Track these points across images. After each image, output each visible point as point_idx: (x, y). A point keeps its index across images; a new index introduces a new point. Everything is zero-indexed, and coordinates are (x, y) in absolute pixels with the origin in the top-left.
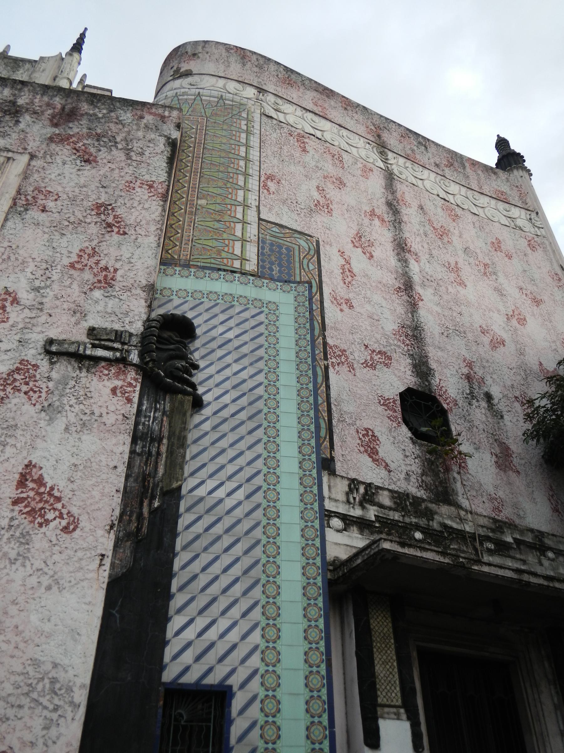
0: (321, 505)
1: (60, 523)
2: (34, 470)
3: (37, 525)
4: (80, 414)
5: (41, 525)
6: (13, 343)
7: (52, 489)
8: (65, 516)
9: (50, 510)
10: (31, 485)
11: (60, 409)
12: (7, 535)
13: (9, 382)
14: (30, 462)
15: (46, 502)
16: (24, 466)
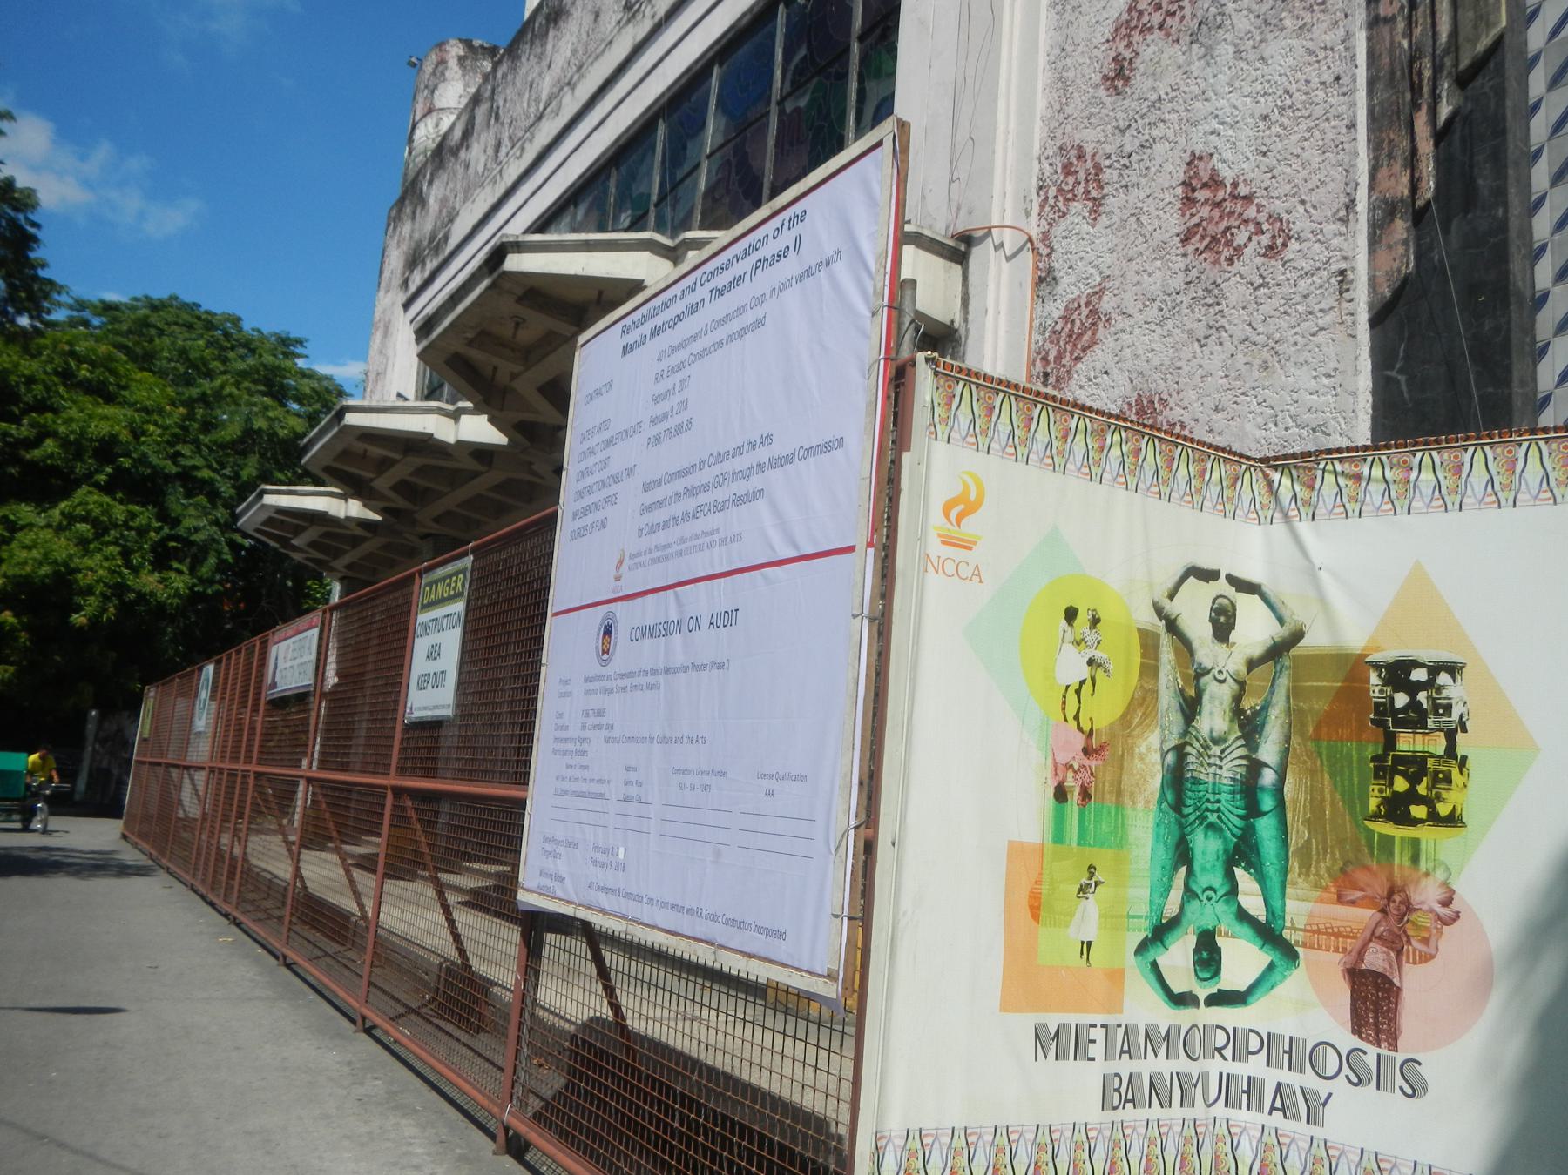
3: (1225, 264)
5: (1230, 261)
7: (1235, 185)
8: (1265, 227)
10: (1201, 195)
12: (1186, 300)
13: (1133, 24)
14: (1193, 153)
15: (1231, 213)
16: (1184, 167)
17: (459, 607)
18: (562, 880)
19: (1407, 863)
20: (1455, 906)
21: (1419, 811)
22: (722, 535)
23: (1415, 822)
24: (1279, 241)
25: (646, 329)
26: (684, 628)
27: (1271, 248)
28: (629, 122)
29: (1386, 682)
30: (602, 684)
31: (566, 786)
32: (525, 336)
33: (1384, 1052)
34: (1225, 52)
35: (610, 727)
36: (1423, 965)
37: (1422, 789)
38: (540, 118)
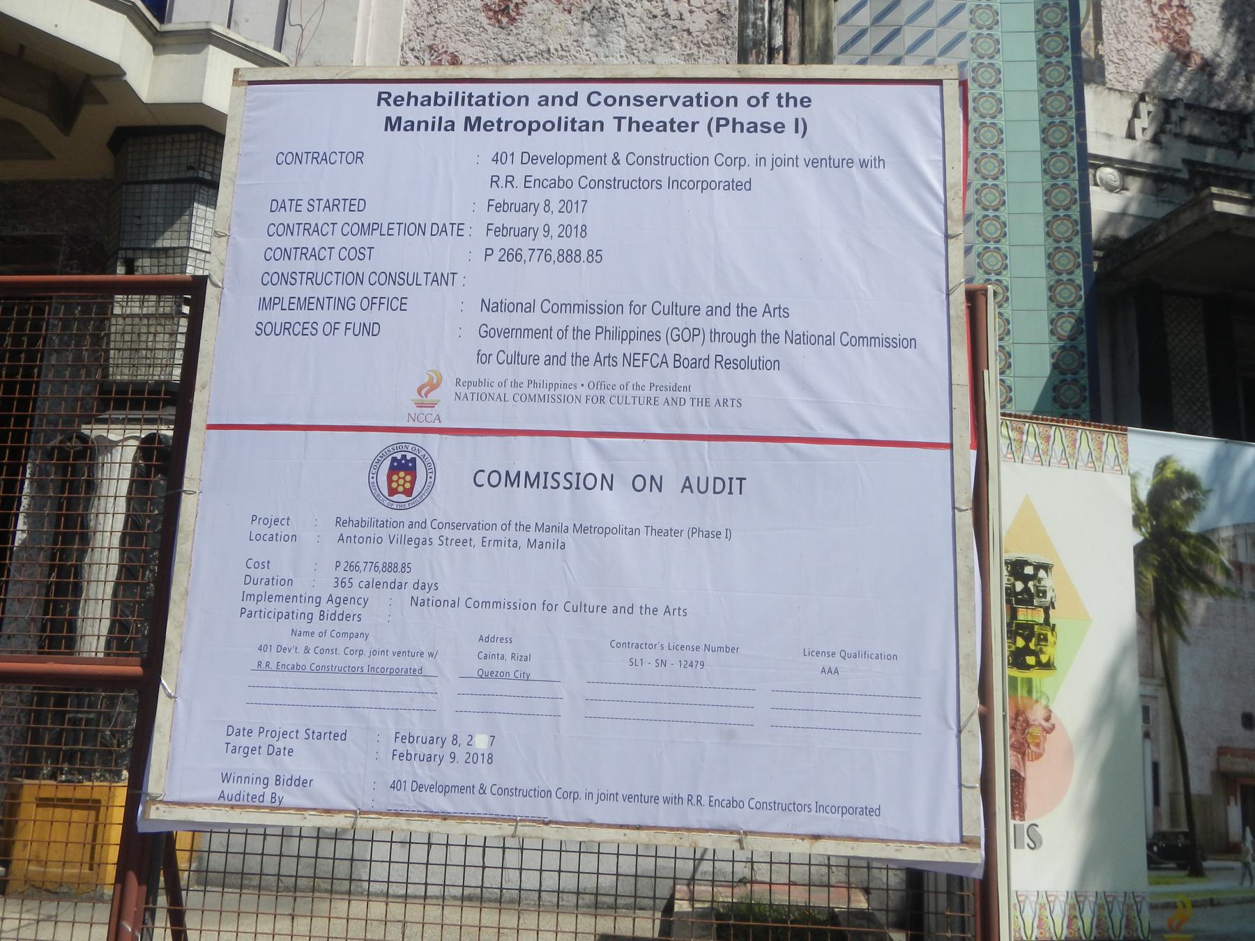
0: (1082, 147)
4: (646, 19)
11: (612, 12)
18: (302, 783)
19: (1025, 694)
20: (1053, 721)
21: (1031, 660)
22: (697, 393)
23: (1029, 667)
25: (457, 114)
29: (1011, 574)
30: (393, 531)
33: (1018, 822)
36: (1036, 762)
37: (1032, 646)
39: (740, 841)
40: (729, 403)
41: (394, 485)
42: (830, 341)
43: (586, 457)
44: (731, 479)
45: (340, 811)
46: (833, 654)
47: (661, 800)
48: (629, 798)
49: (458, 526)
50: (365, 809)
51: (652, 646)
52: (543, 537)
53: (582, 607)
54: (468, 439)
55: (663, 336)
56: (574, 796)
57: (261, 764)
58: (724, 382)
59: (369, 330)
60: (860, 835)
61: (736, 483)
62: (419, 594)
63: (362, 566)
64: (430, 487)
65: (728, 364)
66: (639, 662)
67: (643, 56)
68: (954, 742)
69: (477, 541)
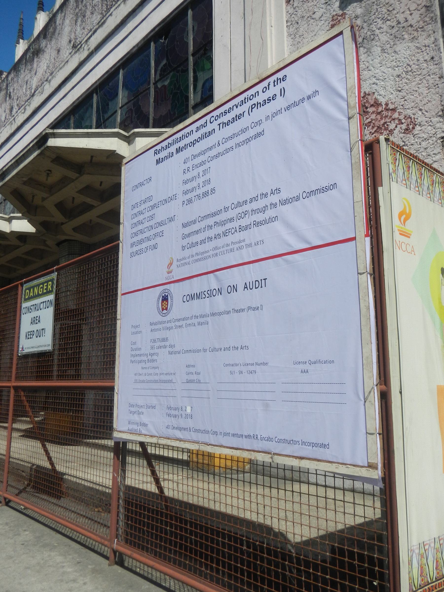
1: (401, 128)
2: (369, 97)
4: (389, 31)
6: (323, 8)
7: (387, 104)
8: (403, 121)
9: (390, 122)
10: (370, 110)
11: (372, 36)
15: (386, 117)
17: (51, 297)
18: (145, 425)
22: (247, 242)
24: (411, 127)
25: (173, 149)
26: (224, 292)
27: (407, 129)
28: (79, 95)
30: (164, 325)
31: (142, 378)
32: (52, 180)
34: (377, 50)
35: (171, 346)
38: (33, 95)
39: (272, 458)
40: (259, 243)
41: (163, 307)
42: (297, 199)
43: (211, 282)
44: (261, 280)
45: (155, 436)
46: (306, 362)
47: (244, 437)
48: (234, 435)
49: (179, 320)
50: (161, 436)
51: (237, 365)
52: (202, 320)
53: (214, 350)
54: (181, 283)
55: (235, 218)
56: (215, 433)
57: (136, 418)
58: (255, 234)
59: (155, 247)
60: (321, 459)
61: (263, 281)
62: (171, 350)
63: (156, 340)
64: (172, 305)
65: (257, 224)
66: (233, 373)
67: (390, 51)
68: (363, 407)
69: (184, 326)
